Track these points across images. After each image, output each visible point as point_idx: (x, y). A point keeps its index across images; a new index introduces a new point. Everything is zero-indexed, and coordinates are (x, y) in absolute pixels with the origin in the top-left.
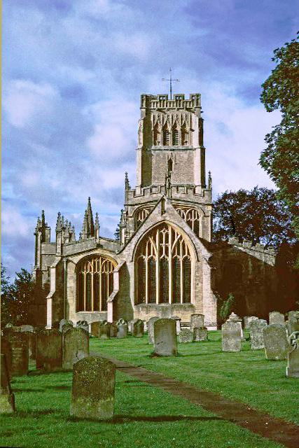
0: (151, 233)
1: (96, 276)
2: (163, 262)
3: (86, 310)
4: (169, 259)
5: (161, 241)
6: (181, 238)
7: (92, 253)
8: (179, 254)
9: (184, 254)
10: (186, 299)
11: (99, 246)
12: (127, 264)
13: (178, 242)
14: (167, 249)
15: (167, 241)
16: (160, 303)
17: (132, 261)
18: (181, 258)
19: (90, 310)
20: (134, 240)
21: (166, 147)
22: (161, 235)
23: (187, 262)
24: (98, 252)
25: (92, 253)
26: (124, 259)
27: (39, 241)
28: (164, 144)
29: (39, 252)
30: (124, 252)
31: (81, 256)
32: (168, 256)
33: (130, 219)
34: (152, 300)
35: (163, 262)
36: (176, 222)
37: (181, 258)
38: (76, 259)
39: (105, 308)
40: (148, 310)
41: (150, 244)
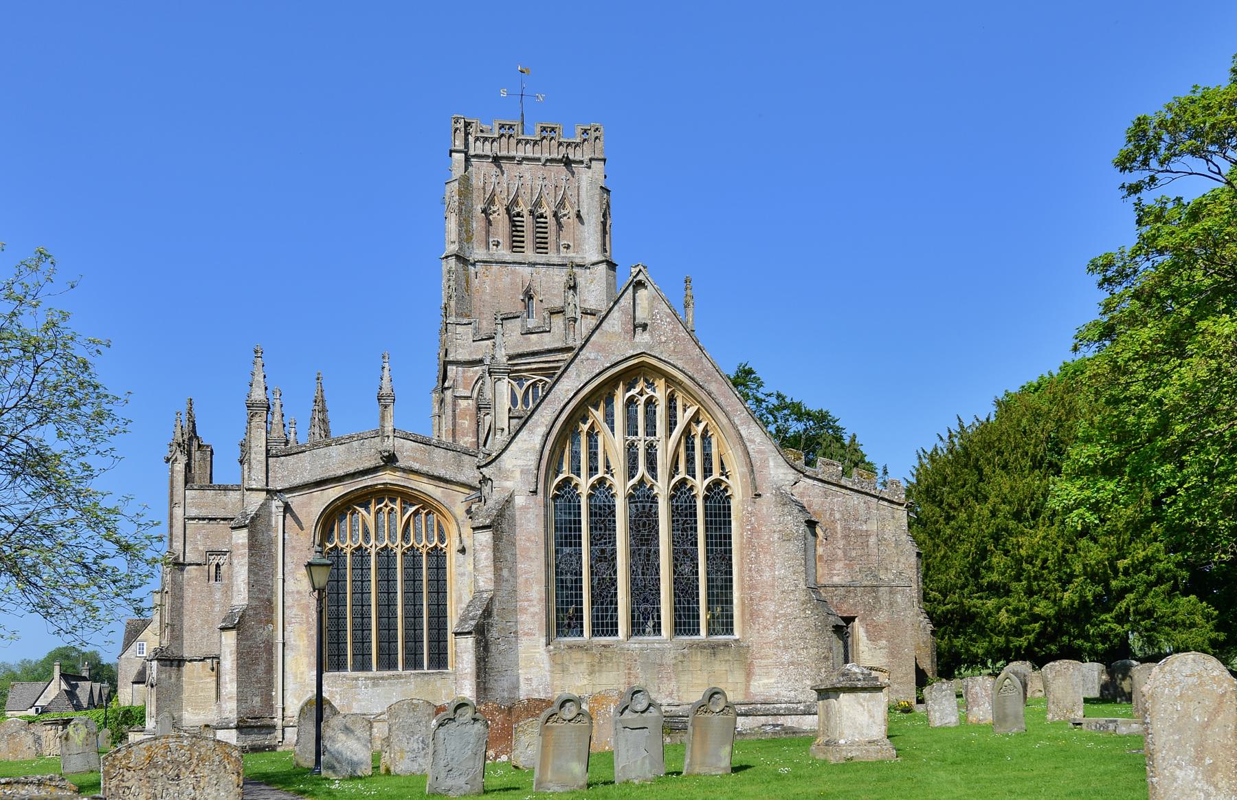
0: (601, 394)
1: (386, 555)
2: (642, 501)
3: (354, 669)
4: (662, 488)
5: (631, 428)
6: (696, 419)
7: (368, 481)
8: (691, 471)
9: (707, 471)
10: (723, 623)
11: (390, 460)
12: (519, 500)
13: (687, 433)
14: (651, 448)
15: (651, 429)
16: (629, 637)
17: (535, 492)
18: (700, 485)
19: (392, 665)
20: (544, 417)
21: (518, 257)
22: (631, 402)
23: (718, 498)
24: (387, 477)
25: (368, 481)
26: (509, 484)
27: (180, 478)
28: (516, 244)
29: (178, 512)
30: (508, 461)
31: (334, 492)
32: (655, 477)
33: (463, 404)
34: (605, 625)
35: (642, 501)
36: (680, 364)
37: (700, 485)
38: (313, 505)
39: (439, 659)
40: (600, 661)
41: (592, 435)
